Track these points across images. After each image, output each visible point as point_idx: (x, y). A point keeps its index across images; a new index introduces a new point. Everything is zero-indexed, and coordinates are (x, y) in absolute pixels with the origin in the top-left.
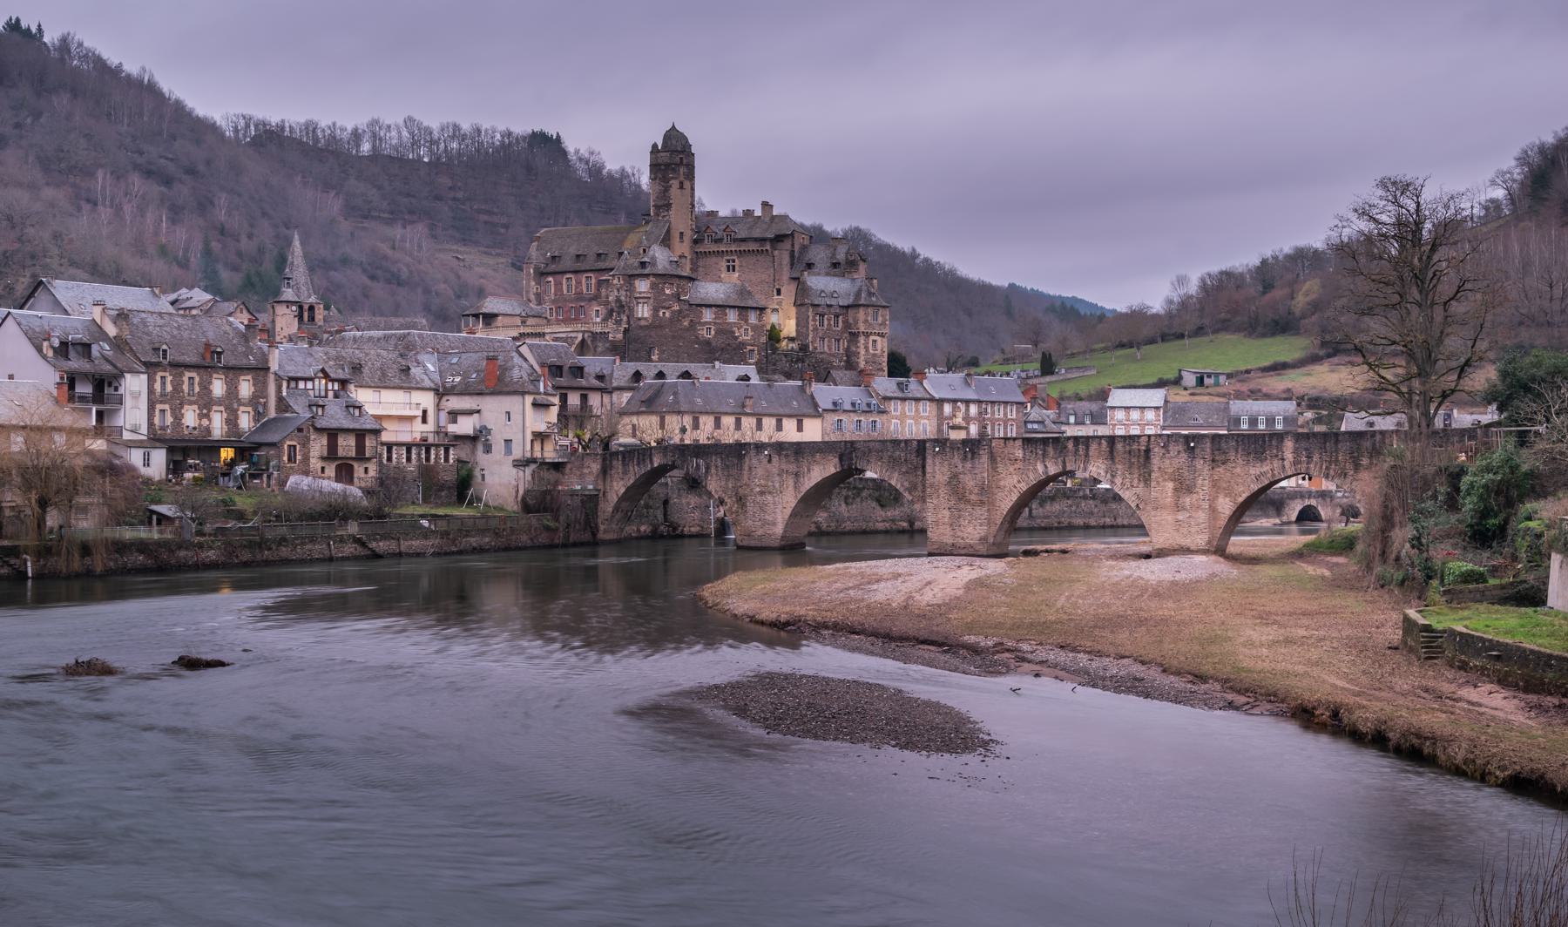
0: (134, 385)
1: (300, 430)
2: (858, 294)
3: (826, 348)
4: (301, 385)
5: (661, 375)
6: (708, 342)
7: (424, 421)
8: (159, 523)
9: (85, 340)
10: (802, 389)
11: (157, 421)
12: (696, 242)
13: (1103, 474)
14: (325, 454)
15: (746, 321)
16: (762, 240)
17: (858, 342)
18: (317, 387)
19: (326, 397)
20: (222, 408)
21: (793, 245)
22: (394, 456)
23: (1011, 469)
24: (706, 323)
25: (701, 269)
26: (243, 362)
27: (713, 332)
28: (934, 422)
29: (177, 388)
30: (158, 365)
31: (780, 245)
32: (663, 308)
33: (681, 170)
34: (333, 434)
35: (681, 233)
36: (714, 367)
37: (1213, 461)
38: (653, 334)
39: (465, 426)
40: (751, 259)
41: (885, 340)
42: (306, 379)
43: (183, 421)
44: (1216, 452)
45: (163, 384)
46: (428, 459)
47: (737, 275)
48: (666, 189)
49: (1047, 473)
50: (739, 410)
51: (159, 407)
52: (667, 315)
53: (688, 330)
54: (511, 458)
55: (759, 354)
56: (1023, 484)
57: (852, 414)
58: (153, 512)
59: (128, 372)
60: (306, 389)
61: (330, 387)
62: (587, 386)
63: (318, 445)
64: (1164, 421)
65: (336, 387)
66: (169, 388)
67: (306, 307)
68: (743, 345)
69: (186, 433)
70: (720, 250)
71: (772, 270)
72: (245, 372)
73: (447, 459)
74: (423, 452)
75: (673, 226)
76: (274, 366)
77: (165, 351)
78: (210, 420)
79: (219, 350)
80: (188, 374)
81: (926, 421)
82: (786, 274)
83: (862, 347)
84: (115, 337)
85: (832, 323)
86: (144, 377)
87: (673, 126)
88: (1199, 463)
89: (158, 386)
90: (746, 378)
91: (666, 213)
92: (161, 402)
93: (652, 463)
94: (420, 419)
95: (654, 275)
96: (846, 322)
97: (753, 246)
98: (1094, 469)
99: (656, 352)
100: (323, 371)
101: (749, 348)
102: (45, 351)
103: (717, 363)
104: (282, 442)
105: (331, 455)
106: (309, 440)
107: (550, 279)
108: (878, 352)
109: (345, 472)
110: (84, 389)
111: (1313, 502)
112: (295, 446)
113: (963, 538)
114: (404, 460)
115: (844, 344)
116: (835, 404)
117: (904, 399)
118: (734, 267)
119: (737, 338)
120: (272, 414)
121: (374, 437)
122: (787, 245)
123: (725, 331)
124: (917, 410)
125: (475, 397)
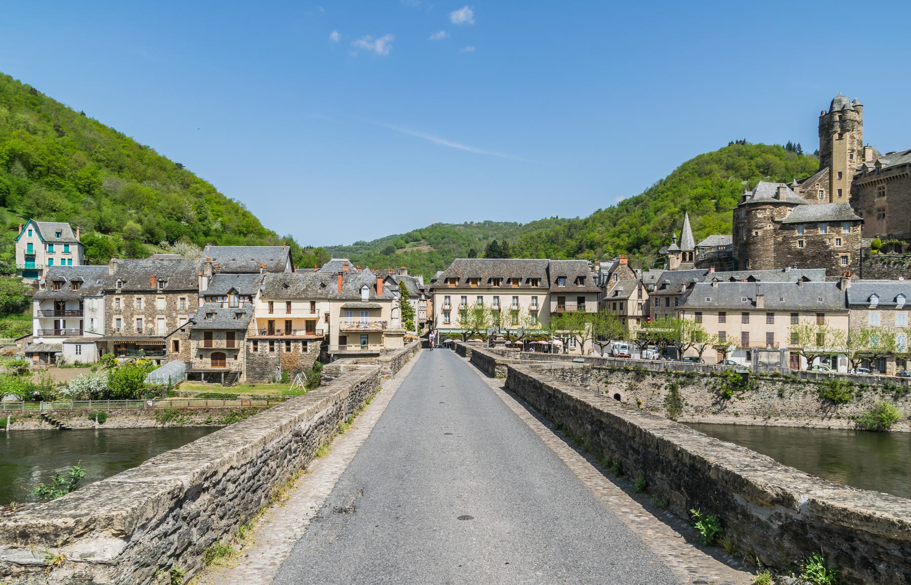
6: (800, 253)
15: (839, 233)
20: (164, 316)
22: (259, 347)
25: (861, 198)
32: (756, 228)
34: (208, 335)
47: (885, 198)
51: (115, 317)
53: (780, 244)
55: (853, 259)
68: (836, 252)
78: (154, 324)
80: (136, 296)
100: (233, 289)
101: (841, 254)
110: (52, 307)
118: (884, 192)
119: (828, 247)
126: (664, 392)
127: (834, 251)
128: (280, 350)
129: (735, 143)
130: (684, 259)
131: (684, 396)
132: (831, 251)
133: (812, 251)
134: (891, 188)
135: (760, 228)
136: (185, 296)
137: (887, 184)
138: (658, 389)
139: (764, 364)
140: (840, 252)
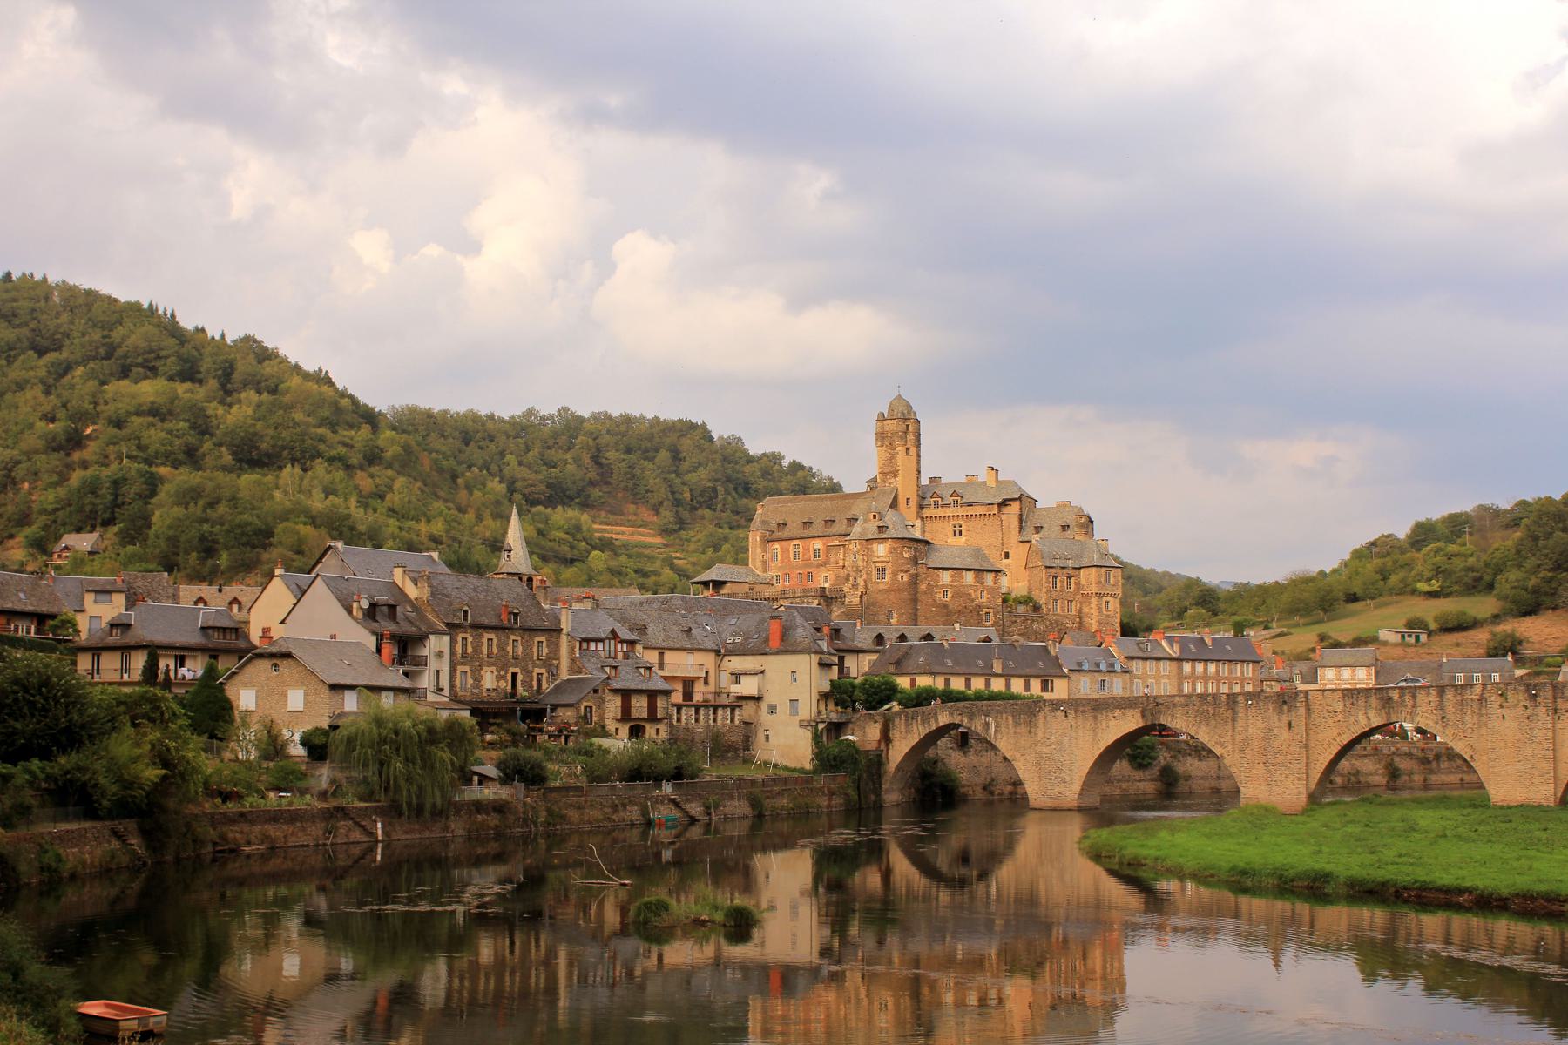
0: (437, 645)
1: (595, 691)
4: (593, 646)
5: (902, 638)
6: (945, 606)
7: (706, 683)
8: (480, 783)
9: (391, 602)
11: (458, 682)
13: (1432, 724)
14: (619, 716)
15: (982, 584)
16: (991, 504)
17: (1090, 603)
18: (607, 648)
19: (615, 658)
22: (684, 717)
23: (1330, 721)
24: (943, 586)
26: (539, 624)
27: (949, 595)
28: (1175, 682)
29: (477, 649)
30: (459, 626)
31: (1006, 510)
32: (902, 571)
34: (626, 694)
35: (908, 499)
37: (1555, 711)
39: (748, 687)
41: (1118, 601)
42: (597, 641)
43: (482, 683)
44: (1559, 700)
45: (464, 645)
46: (715, 720)
47: (963, 539)
48: (893, 457)
49: (1369, 725)
51: (460, 668)
52: (905, 579)
54: (798, 718)
55: (995, 616)
56: (1344, 736)
57: (1096, 674)
58: (476, 773)
59: (432, 633)
60: (596, 650)
61: (619, 648)
62: (845, 648)
63: (613, 705)
65: (625, 649)
66: (470, 650)
68: (979, 607)
69: (485, 694)
71: (1000, 534)
72: (539, 633)
73: (732, 720)
74: (711, 712)
76: (565, 625)
77: (466, 612)
79: (516, 611)
80: (487, 636)
81: (1167, 681)
82: (1014, 536)
84: (416, 599)
86: (447, 639)
88: (1541, 710)
89: (459, 648)
90: (990, 641)
91: (893, 480)
92: (462, 664)
93: (937, 721)
94: (702, 680)
98: (1422, 720)
99: (895, 615)
101: (985, 610)
102: (355, 613)
104: (579, 702)
105: (625, 715)
106: (604, 701)
107: (776, 546)
109: (636, 731)
112: (591, 708)
113: (1279, 793)
114: (693, 721)
117: (1146, 659)
118: (960, 532)
119: (973, 601)
120: (564, 675)
121: (664, 698)
124: (1158, 670)
125: (759, 657)
128: (724, 719)
134: (971, 529)
136: (543, 639)
137: (965, 522)
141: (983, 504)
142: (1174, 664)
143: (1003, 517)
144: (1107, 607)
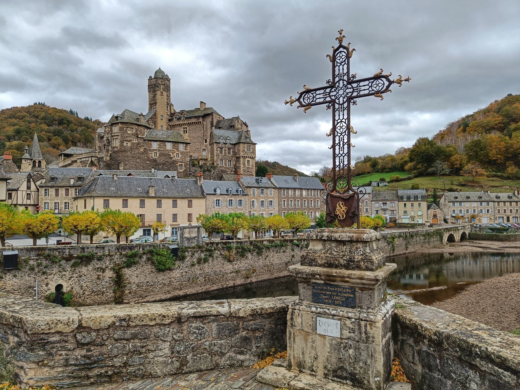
2: (240, 138)
3: (224, 165)
6: (155, 160)
10: (196, 182)
12: (170, 120)
15: (178, 149)
17: (240, 161)
21: (212, 119)
24: (154, 150)
27: (158, 155)
32: (126, 141)
33: (162, 87)
36: (151, 172)
38: (120, 155)
40: (194, 127)
47: (187, 134)
48: (155, 96)
50: (145, 195)
55: (185, 166)
57: (226, 196)
64: (372, 199)
67: (37, 161)
70: (180, 123)
75: (158, 112)
83: (242, 163)
85: (227, 152)
87: (160, 69)
91: (155, 107)
95: (122, 123)
96: (234, 152)
97: (194, 120)
99: (122, 165)
101: (179, 163)
103: (153, 170)
108: (251, 166)
111: (452, 232)
115: (233, 163)
116: (227, 191)
118: (186, 131)
119: (171, 158)
122: (209, 119)
123: (165, 154)
126: (109, 274)
127: (176, 161)
129: (38, 104)
130: (34, 166)
131: (127, 276)
132: (174, 161)
133: (162, 160)
135: (130, 141)
138: (103, 272)
139: (188, 239)
140: (179, 162)
141: (195, 117)
142: (276, 191)
143: (204, 123)
144: (249, 165)
